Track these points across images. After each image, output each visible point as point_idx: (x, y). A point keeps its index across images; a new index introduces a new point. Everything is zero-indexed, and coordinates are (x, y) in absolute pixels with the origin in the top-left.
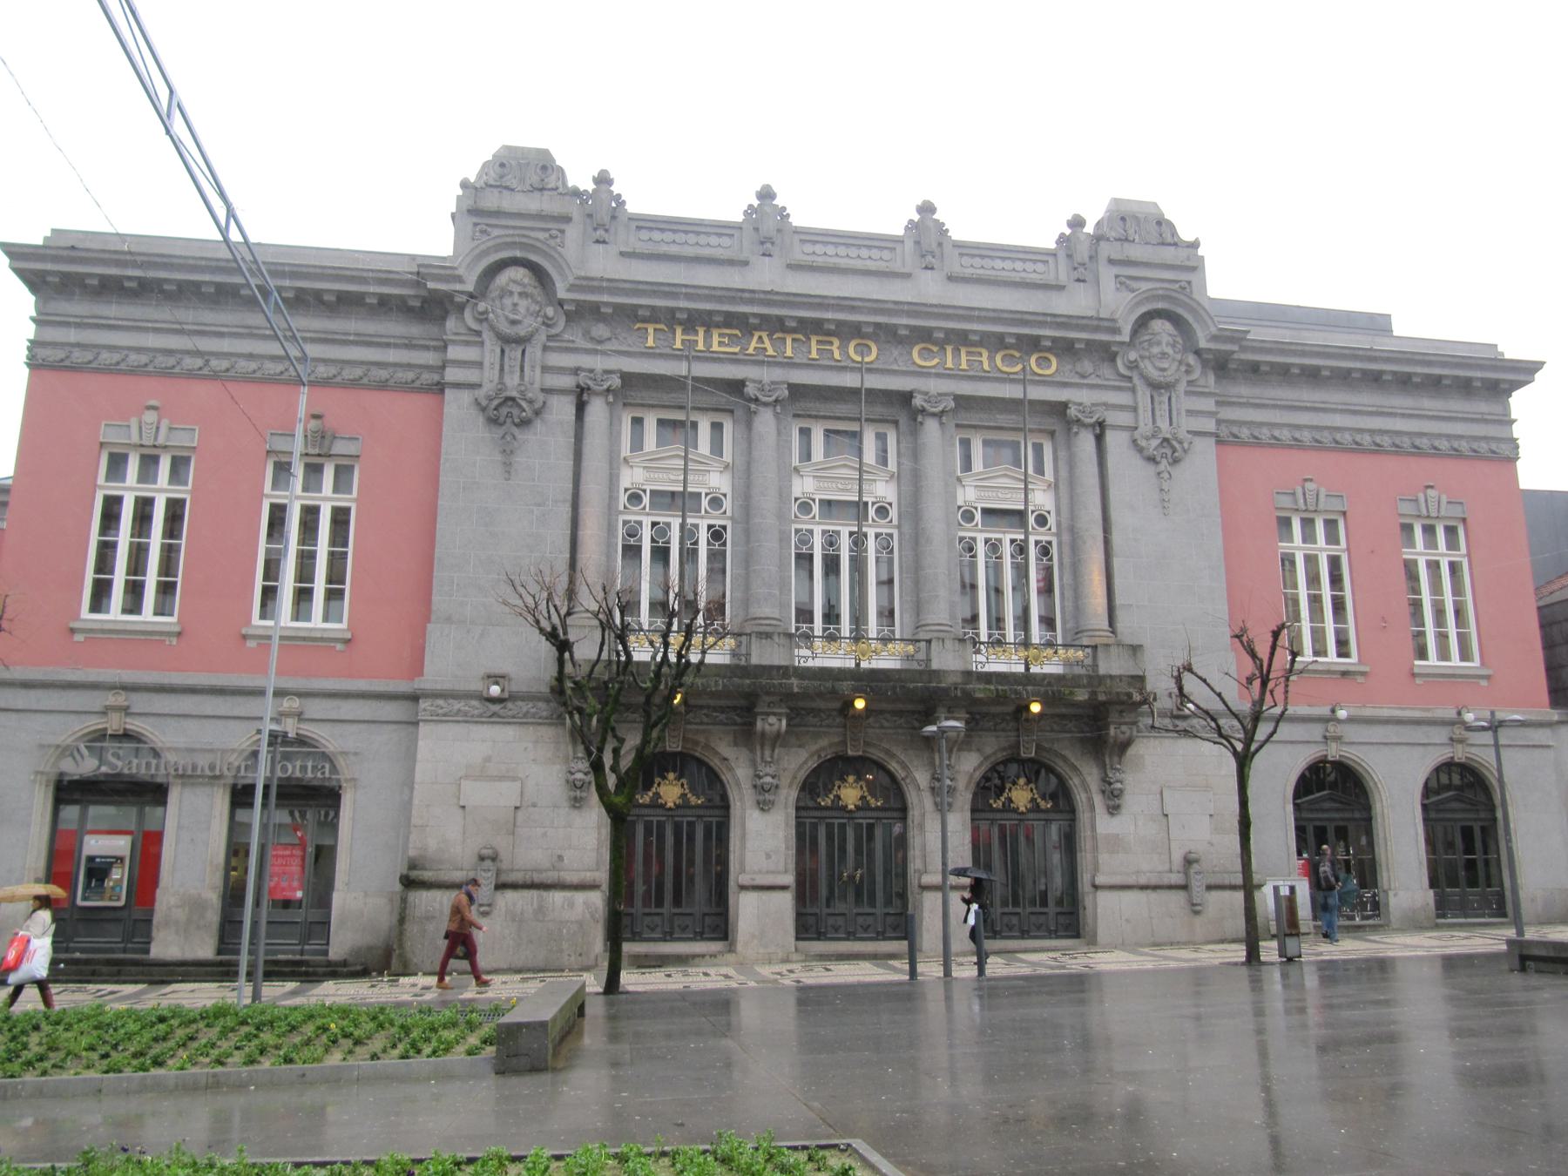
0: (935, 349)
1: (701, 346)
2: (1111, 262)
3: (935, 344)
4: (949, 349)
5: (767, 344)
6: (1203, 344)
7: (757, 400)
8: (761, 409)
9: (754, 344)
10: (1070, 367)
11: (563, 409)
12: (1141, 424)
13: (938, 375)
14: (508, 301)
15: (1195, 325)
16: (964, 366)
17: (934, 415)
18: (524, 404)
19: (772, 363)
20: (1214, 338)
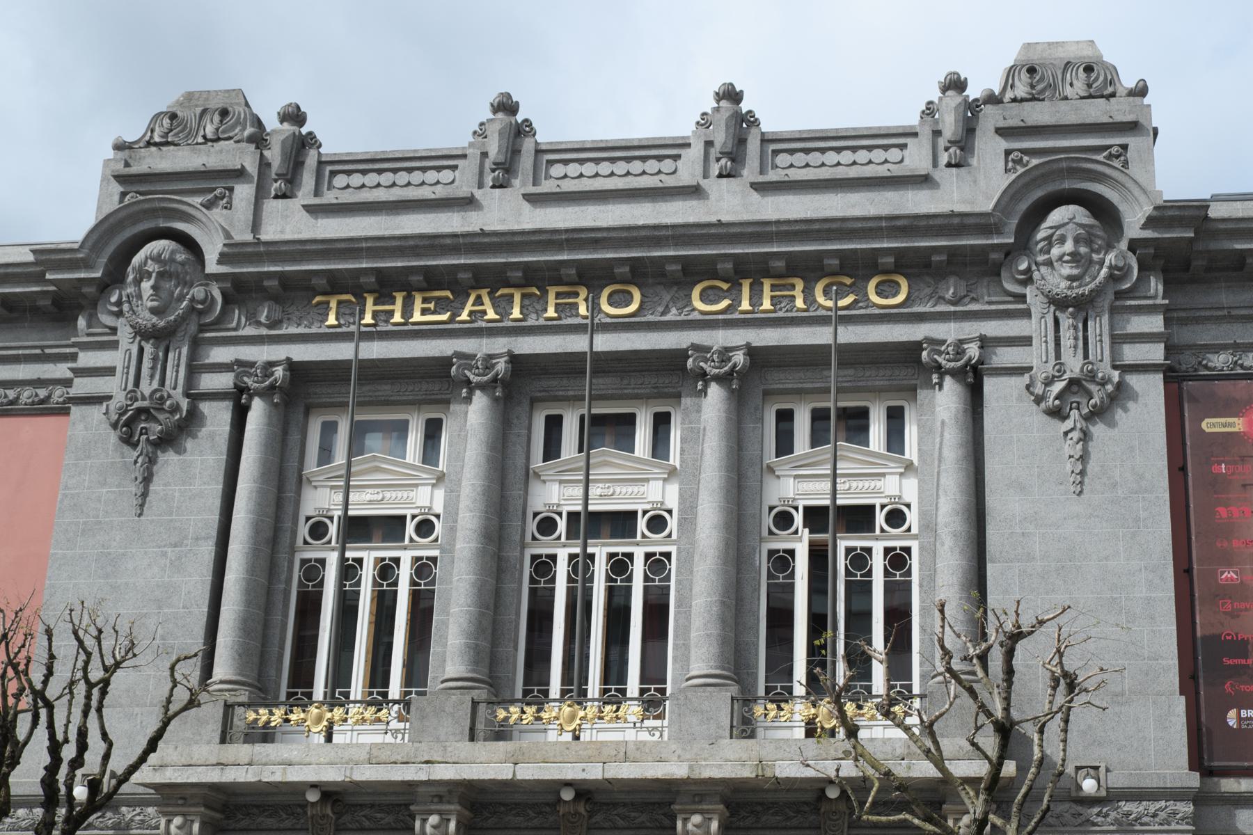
0: (725, 286)
3: (726, 281)
10: (928, 291)
11: (218, 417)
14: (146, 286)
16: (767, 304)
18: (161, 417)
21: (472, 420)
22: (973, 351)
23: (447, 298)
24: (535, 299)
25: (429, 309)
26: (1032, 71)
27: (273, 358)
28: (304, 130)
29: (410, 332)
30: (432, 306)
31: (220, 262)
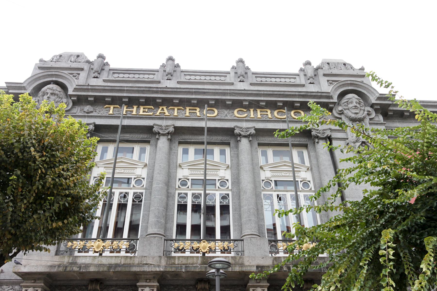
0: (245, 110)
1: (134, 113)
2: (325, 75)
4: (252, 110)
5: (166, 111)
6: (374, 101)
7: (159, 133)
8: (161, 137)
9: (159, 111)
12: (349, 137)
13: (247, 121)
14: (46, 97)
15: (368, 95)
16: (259, 116)
17: (245, 137)
19: (167, 118)
20: (379, 98)
21: (163, 142)
22: (328, 133)
23: (152, 108)
24: (181, 110)
25: (145, 111)
26: (328, 64)
27: (89, 122)
28: (105, 61)
29: (139, 116)
30: (146, 110)
31: (73, 91)
